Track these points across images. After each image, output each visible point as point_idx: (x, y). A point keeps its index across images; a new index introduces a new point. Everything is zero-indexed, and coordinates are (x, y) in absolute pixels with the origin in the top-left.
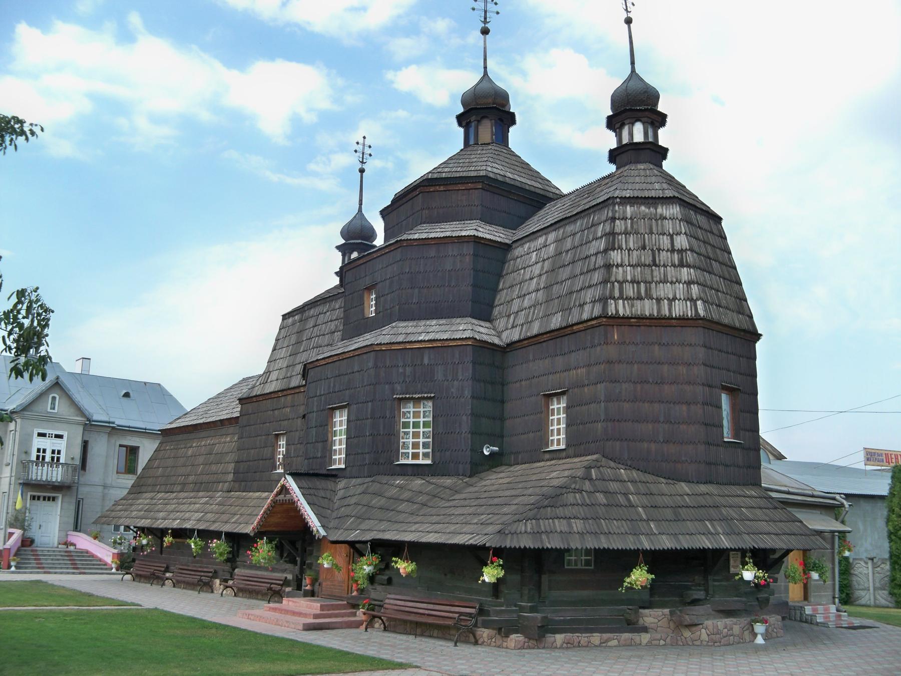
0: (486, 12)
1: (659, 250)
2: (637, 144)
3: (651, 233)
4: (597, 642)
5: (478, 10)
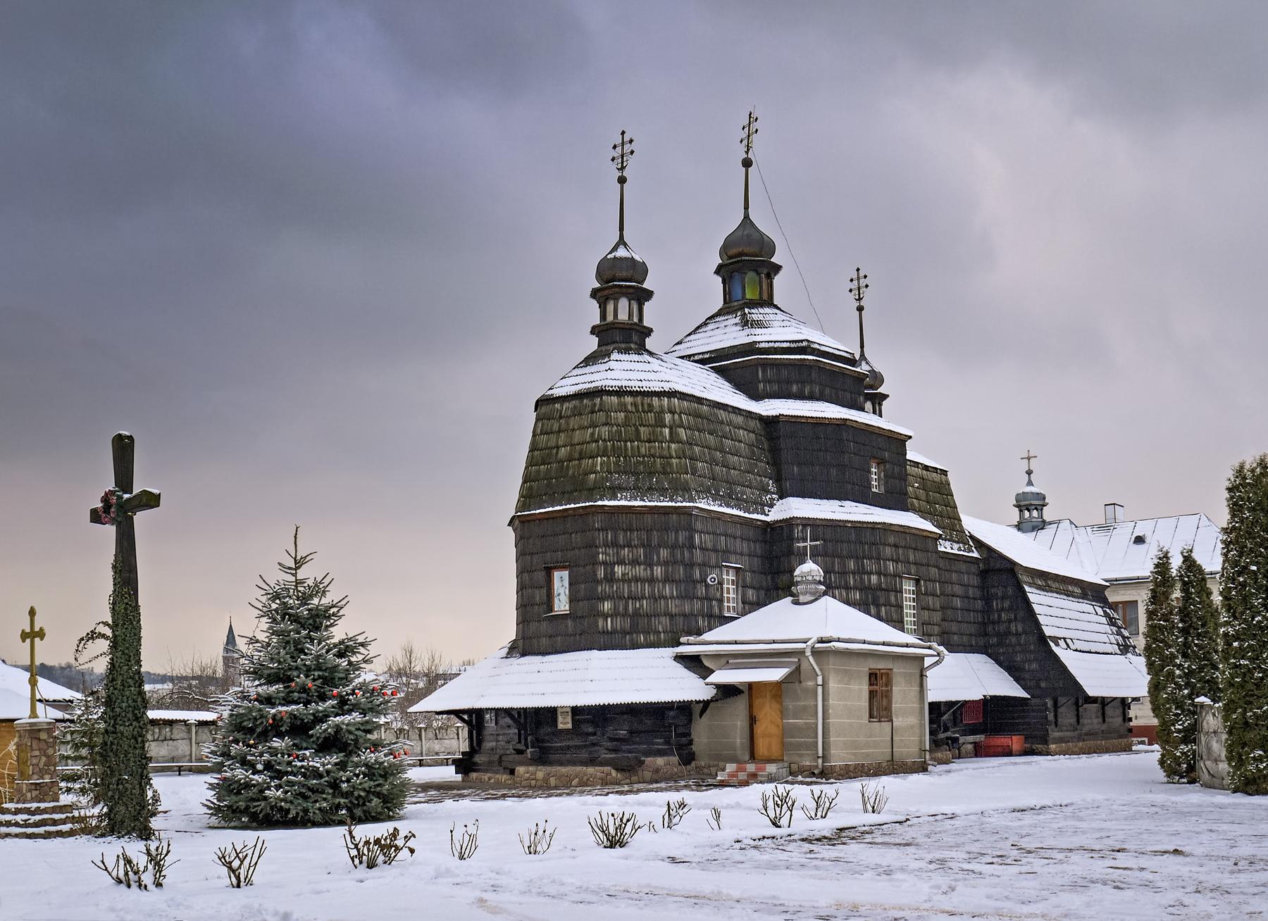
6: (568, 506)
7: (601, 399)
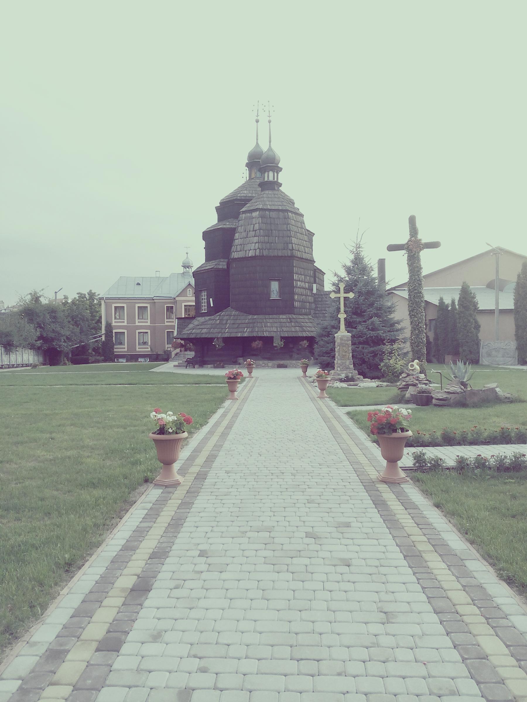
1: (249, 231)
7: (288, 213)
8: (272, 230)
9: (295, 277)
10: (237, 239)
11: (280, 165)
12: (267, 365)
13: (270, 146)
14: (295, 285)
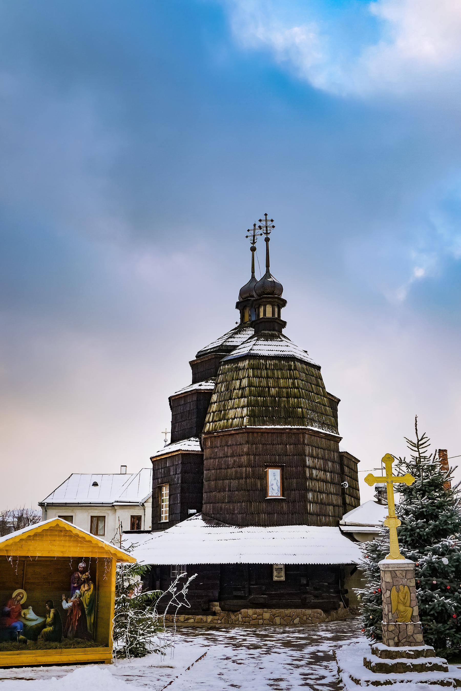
0: (254, 236)
2: (269, 318)
3: (233, 380)
4: (182, 620)
5: (250, 236)
6: (286, 427)
8: (269, 388)
9: (309, 461)
10: (214, 403)
11: (283, 296)
12: (261, 617)
13: (268, 271)
14: (308, 475)
